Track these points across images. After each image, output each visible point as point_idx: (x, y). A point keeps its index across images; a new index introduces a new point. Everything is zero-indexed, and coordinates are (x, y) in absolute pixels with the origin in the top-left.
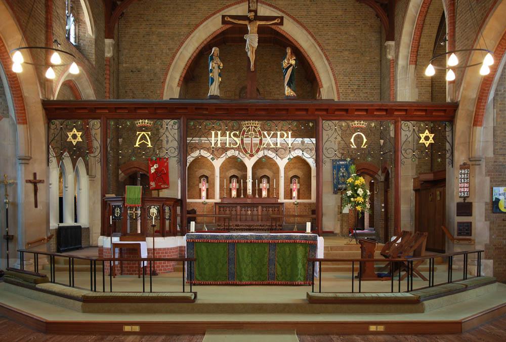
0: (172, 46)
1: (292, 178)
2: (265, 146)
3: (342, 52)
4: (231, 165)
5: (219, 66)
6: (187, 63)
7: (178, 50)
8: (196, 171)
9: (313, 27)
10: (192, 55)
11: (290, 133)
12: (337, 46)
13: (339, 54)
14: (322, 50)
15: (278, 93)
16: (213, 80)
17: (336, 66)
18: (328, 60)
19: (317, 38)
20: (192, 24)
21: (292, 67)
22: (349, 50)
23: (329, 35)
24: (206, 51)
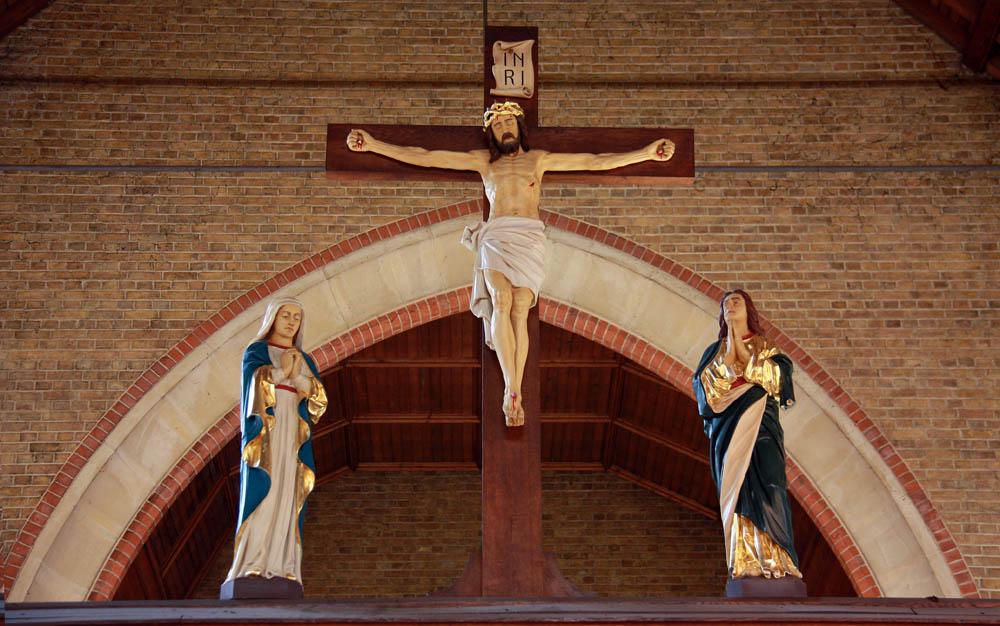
0: (50, 435)
5: (303, 405)
6: (133, 526)
7: (86, 453)
9: (816, 333)
10: (168, 480)
12: (956, 424)
13: (976, 466)
14: (879, 444)
16: (261, 484)
17: (968, 529)
18: (916, 495)
19: (851, 386)
20: (175, 324)
21: (763, 400)
23: (909, 373)
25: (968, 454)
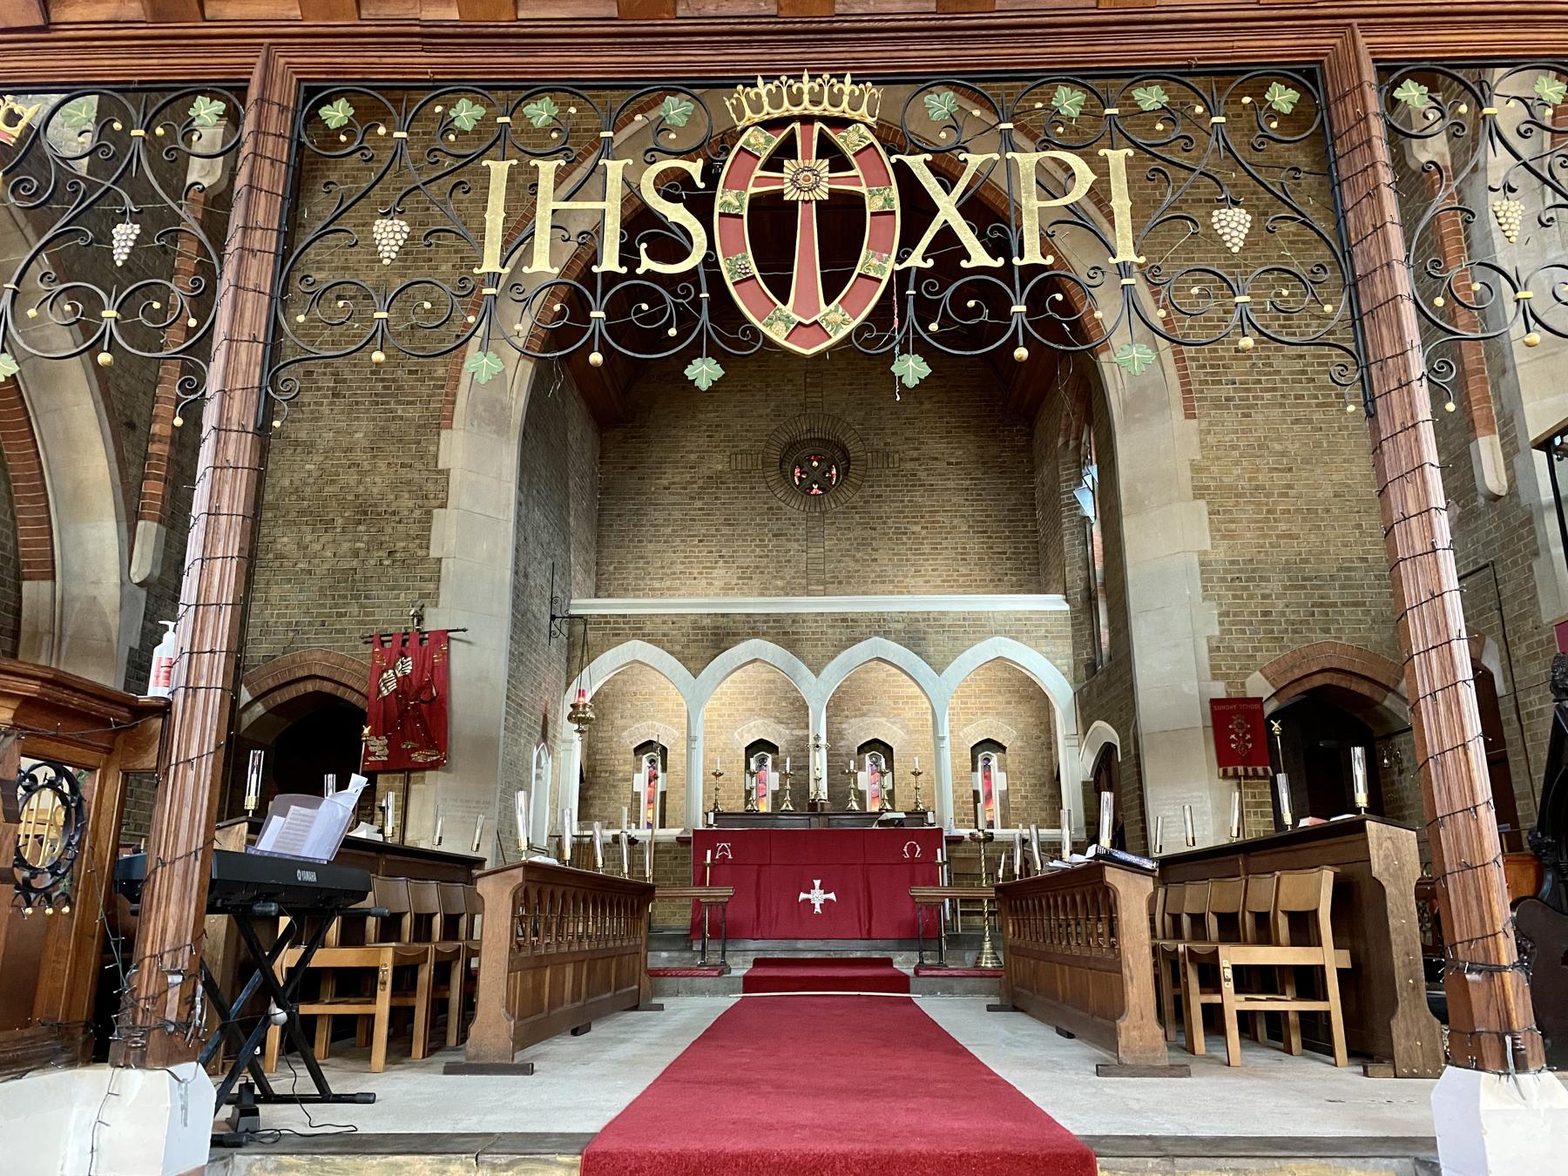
1: (975, 749)
2: (916, 260)
4: (751, 704)
8: (624, 728)
11: (1117, 158)
15: (915, 454)
22: (1207, 201)
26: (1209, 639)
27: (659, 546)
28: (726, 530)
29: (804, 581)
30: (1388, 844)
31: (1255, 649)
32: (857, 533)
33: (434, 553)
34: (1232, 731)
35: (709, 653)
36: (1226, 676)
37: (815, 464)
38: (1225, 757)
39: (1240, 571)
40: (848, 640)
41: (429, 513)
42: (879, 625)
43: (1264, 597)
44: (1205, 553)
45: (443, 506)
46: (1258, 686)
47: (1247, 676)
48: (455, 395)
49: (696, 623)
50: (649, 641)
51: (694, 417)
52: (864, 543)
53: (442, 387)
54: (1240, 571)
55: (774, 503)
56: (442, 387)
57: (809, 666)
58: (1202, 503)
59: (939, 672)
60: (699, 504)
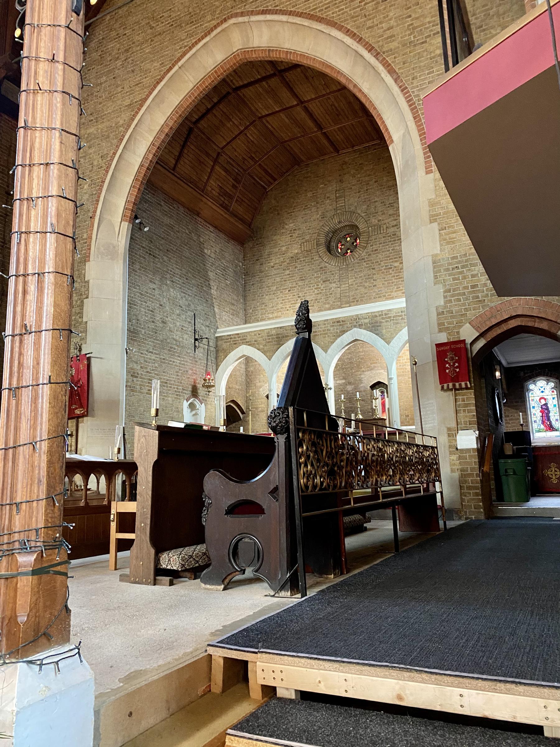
3: (426, 42)
8: (261, 387)
12: (409, 35)
13: (419, 49)
19: (365, 35)
23: (391, 19)
24: (269, 186)
25: (415, 45)
26: (437, 308)
27: (271, 297)
28: (300, 283)
29: (339, 303)
30: (143, 440)
31: (466, 310)
32: (365, 272)
33: (84, 320)
34: (447, 362)
35: (276, 347)
36: (448, 328)
37: (348, 239)
38: (443, 378)
39: (457, 263)
40: (340, 332)
41: (82, 302)
42: (356, 322)
43: (473, 276)
44: (436, 255)
45: (87, 298)
46: (468, 333)
47: (460, 327)
48: (90, 245)
49: (269, 333)
50: (249, 345)
51: (283, 228)
52: (369, 277)
53: (86, 243)
54: (457, 263)
55: (323, 265)
56: (86, 243)
57: (322, 348)
58: (435, 225)
59: (388, 343)
60: (288, 272)
